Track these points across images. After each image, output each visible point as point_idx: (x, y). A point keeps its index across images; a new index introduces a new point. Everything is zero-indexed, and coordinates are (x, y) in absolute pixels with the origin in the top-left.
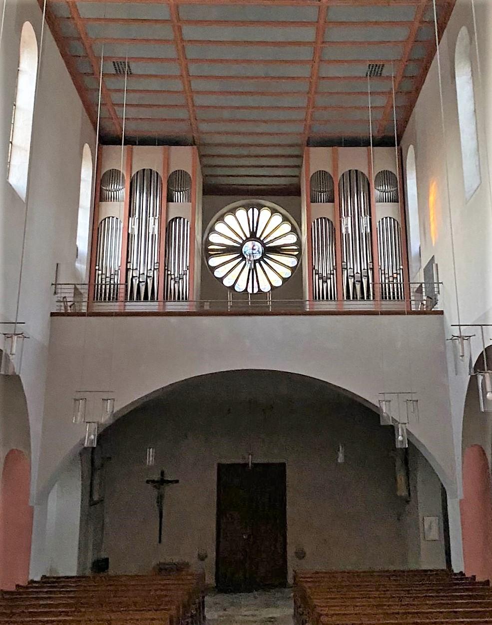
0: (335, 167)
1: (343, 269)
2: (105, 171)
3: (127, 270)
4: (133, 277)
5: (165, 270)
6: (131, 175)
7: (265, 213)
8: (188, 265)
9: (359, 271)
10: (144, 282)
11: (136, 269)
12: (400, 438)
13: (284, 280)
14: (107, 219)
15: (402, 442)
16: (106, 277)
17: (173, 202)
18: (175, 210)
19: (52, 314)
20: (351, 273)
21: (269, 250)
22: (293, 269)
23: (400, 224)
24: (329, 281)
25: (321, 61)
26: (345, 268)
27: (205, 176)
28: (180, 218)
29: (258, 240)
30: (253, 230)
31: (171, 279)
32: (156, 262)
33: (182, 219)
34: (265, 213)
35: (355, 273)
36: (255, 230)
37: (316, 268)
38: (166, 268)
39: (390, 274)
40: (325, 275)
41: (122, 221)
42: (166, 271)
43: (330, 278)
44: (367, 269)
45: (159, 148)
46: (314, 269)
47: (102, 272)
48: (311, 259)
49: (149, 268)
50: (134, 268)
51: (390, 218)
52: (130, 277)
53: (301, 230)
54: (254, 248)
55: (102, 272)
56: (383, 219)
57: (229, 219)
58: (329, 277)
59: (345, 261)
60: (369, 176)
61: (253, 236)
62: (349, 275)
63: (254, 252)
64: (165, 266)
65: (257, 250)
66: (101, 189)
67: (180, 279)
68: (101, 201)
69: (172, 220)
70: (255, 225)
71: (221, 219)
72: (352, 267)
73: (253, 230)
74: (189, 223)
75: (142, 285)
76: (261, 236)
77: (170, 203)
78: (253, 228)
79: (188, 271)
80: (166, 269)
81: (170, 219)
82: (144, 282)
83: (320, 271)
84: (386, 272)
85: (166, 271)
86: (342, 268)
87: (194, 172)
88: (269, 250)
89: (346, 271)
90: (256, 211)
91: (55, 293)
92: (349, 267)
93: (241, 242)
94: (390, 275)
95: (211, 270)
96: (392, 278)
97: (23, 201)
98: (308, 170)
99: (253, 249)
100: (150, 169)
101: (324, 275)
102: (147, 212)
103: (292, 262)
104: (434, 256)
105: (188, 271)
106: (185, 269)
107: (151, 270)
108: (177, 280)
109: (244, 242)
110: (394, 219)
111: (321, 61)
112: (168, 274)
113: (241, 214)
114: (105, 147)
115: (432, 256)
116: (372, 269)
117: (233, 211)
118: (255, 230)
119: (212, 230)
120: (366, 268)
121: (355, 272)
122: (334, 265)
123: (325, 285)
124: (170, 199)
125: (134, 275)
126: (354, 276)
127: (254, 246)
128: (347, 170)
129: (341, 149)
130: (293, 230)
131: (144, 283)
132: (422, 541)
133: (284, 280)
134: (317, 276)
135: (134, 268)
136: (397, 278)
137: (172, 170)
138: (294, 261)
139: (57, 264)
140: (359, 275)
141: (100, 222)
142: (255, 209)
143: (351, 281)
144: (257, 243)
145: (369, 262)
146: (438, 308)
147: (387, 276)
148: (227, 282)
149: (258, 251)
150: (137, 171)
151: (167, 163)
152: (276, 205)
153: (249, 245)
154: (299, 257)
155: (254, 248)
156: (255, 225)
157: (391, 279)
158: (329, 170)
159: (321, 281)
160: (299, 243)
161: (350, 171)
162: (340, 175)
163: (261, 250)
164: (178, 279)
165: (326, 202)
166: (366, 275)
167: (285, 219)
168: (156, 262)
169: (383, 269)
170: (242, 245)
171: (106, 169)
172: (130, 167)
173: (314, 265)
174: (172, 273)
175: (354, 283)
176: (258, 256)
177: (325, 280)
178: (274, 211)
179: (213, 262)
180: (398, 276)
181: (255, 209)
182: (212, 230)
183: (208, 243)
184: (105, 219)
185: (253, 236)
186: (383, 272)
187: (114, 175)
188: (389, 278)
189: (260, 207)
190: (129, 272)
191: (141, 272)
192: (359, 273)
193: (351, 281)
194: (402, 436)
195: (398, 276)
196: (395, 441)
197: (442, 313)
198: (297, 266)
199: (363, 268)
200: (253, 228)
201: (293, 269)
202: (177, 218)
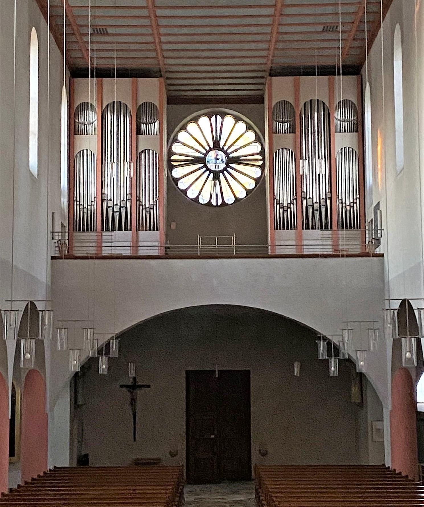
0: (297, 98)
1: (303, 199)
2: (79, 103)
3: (102, 200)
4: (108, 207)
5: (137, 201)
6: (102, 106)
7: (229, 120)
8: (158, 196)
9: (318, 201)
10: (118, 212)
11: (110, 200)
12: (333, 369)
13: (248, 192)
14: (81, 152)
15: (334, 371)
16: (84, 208)
17: (142, 134)
18: (144, 142)
19: (53, 258)
20: (310, 202)
21: (231, 161)
22: (257, 180)
23: (357, 153)
24: (289, 210)
25: (281, 15)
26: (304, 198)
27: (168, 91)
28: (150, 150)
29: (222, 150)
30: (216, 138)
31: (142, 209)
32: (128, 193)
33: (151, 151)
34: (229, 120)
35: (314, 202)
36: (218, 139)
37: (278, 198)
38: (138, 198)
39: (348, 203)
40: (285, 204)
41: (96, 154)
42: (138, 202)
43: (291, 208)
44: (326, 198)
45: (127, 81)
46: (276, 199)
47: (80, 203)
48: (273, 191)
49: (122, 199)
50: (109, 199)
51: (349, 148)
52: (105, 207)
53: (264, 139)
54: (218, 157)
55: (80, 203)
56: (341, 149)
57: (192, 127)
58: (290, 206)
59: (305, 191)
60: (330, 105)
61: (216, 145)
62: (308, 204)
63: (218, 161)
64: (137, 197)
65: (220, 160)
66: (75, 122)
67: (150, 208)
68: (75, 134)
69: (142, 152)
70: (218, 134)
71: (184, 128)
72: (311, 197)
73: (216, 138)
74: (157, 154)
75: (117, 215)
76: (223, 146)
77: (140, 136)
78: (216, 135)
79: (158, 201)
80: (138, 200)
81: (140, 151)
82: (118, 212)
83: (281, 201)
84: (344, 201)
85: (138, 202)
86: (302, 198)
87: (161, 104)
88: (231, 161)
89: (305, 201)
90: (219, 117)
91: (53, 239)
92: (308, 197)
93: (204, 152)
94: (347, 205)
95: (174, 182)
96: (349, 207)
97: (35, 178)
98: (270, 101)
99: (217, 159)
100: (120, 102)
101: (284, 205)
102: (118, 144)
103: (256, 173)
104: (379, 203)
105: (158, 201)
106: (154, 200)
107: (123, 200)
108: (148, 210)
109: (208, 152)
110: (352, 149)
111: (281, 15)
112: (139, 205)
113: (204, 121)
114: (76, 80)
115: (378, 202)
116: (331, 199)
117: (195, 120)
118: (218, 139)
119: (175, 140)
120: (324, 198)
121: (315, 201)
122: (295, 195)
123: (285, 214)
124: (139, 132)
125: (109, 205)
126: (313, 206)
127: (218, 155)
128: (308, 100)
129: (303, 79)
130: (258, 140)
131: (118, 213)
132: (370, 441)
133: (248, 192)
134: (278, 206)
135: (109, 199)
136: (354, 207)
137: (140, 102)
138: (258, 171)
139: (53, 213)
140: (318, 204)
141: (75, 155)
142: (218, 116)
143: (310, 210)
144: (220, 152)
145: (327, 191)
146: (378, 251)
147: (344, 205)
148: (192, 194)
149: (222, 161)
150: (107, 104)
151: (135, 97)
152: (240, 114)
153: (212, 154)
154: (262, 167)
155: (218, 157)
156: (218, 134)
157: (348, 208)
158: (291, 101)
159: (281, 211)
160: (262, 153)
161: (311, 100)
162: (302, 105)
163: (224, 160)
164: (149, 209)
165: (289, 133)
166: (325, 204)
167: (249, 128)
168: (128, 193)
169: (340, 198)
170: (206, 155)
171: (77, 103)
172: (101, 100)
173: (275, 194)
174: (143, 204)
175: (313, 213)
176: (222, 166)
177: (286, 209)
178: (237, 119)
179: (177, 173)
180: (355, 205)
181: (218, 116)
182: (175, 140)
183: (170, 153)
184: (80, 151)
185: (216, 145)
186: (340, 201)
187: (85, 106)
188: (346, 207)
189: (223, 115)
190: (104, 203)
191: (115, 203)
192: (317, 203)
193: (310, 210)
194: (334, 367)
195: (355, 205)
196: (329, 372)
197: (382, 255)
198: (261, 176)
199: (321, 197)
200: (216, 135)
201: (257, 180)
202: (146, 150)
